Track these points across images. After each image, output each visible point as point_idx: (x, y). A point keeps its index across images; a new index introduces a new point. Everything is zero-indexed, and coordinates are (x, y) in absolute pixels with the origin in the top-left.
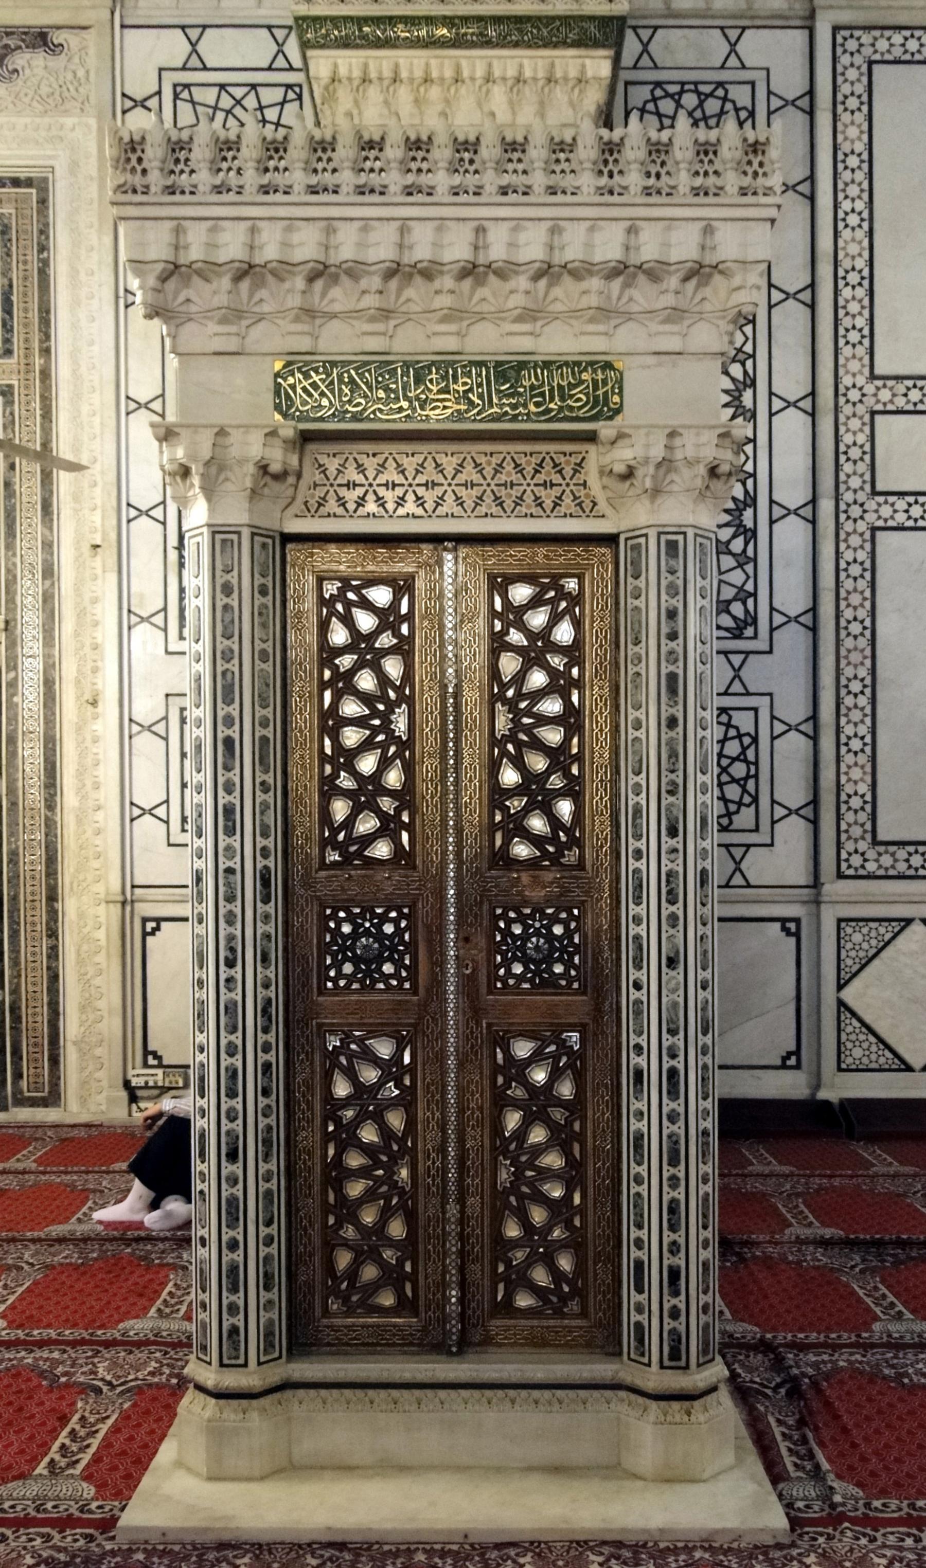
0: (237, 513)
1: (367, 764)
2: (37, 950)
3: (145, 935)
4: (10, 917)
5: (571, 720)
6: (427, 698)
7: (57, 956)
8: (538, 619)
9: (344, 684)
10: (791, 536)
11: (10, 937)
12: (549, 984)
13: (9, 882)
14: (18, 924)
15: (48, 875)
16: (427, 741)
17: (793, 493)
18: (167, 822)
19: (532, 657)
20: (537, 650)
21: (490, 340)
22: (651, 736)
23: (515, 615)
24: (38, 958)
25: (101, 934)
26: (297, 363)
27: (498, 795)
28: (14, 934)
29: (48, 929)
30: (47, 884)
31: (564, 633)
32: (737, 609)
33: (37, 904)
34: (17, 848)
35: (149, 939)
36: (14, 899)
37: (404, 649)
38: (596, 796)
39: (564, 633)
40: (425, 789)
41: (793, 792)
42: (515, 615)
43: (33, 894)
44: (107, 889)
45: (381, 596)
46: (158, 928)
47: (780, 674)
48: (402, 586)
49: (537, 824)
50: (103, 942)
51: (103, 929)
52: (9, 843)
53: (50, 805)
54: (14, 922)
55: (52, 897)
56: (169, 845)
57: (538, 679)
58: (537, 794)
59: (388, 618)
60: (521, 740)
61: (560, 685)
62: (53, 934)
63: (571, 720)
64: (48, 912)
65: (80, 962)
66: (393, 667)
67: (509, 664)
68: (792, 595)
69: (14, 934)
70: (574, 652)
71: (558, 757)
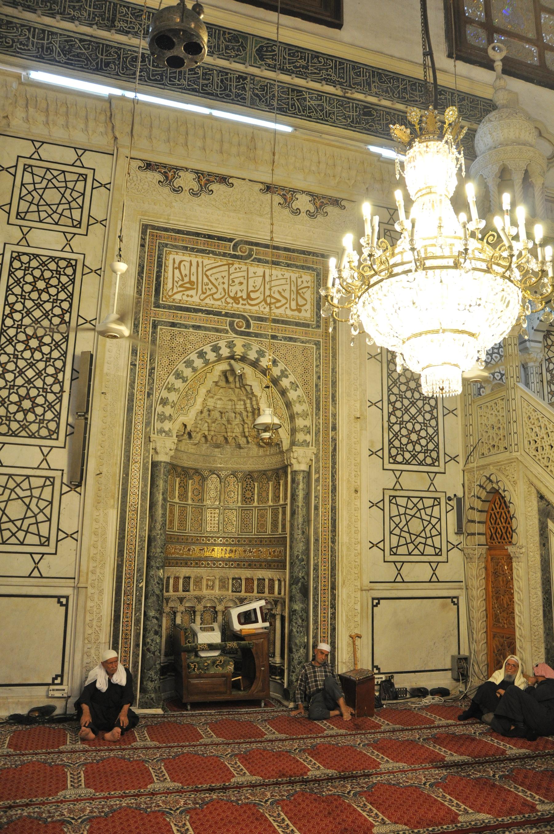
2: (326, 615)
3: (373, 606)
4: (314, 598)
7: (335, 618)
11: (313, 608)
13: (313, 580)
14: (318, 602)
15: (331, 576)
18: (384, 550)
24: (326, 619)
25: (358, 607)
28: (315, 607)
29: (331, 604)
30: (331, 581)
33: (326, 591)
34: (318, 562)
35: (375, 608)
36: (316, 589)
43: (325, 586)
44: (361, 584)
46: (378, 603)
50: (359, 611)
51: (359, 604)
52: (314, 560)
53: (333, 542)
54: (316, 601)
55: (333, 588)
56: (385, 562)
62: (333, 606)
64: (331, 595)
65: (348, 620)
69: (315, 607)
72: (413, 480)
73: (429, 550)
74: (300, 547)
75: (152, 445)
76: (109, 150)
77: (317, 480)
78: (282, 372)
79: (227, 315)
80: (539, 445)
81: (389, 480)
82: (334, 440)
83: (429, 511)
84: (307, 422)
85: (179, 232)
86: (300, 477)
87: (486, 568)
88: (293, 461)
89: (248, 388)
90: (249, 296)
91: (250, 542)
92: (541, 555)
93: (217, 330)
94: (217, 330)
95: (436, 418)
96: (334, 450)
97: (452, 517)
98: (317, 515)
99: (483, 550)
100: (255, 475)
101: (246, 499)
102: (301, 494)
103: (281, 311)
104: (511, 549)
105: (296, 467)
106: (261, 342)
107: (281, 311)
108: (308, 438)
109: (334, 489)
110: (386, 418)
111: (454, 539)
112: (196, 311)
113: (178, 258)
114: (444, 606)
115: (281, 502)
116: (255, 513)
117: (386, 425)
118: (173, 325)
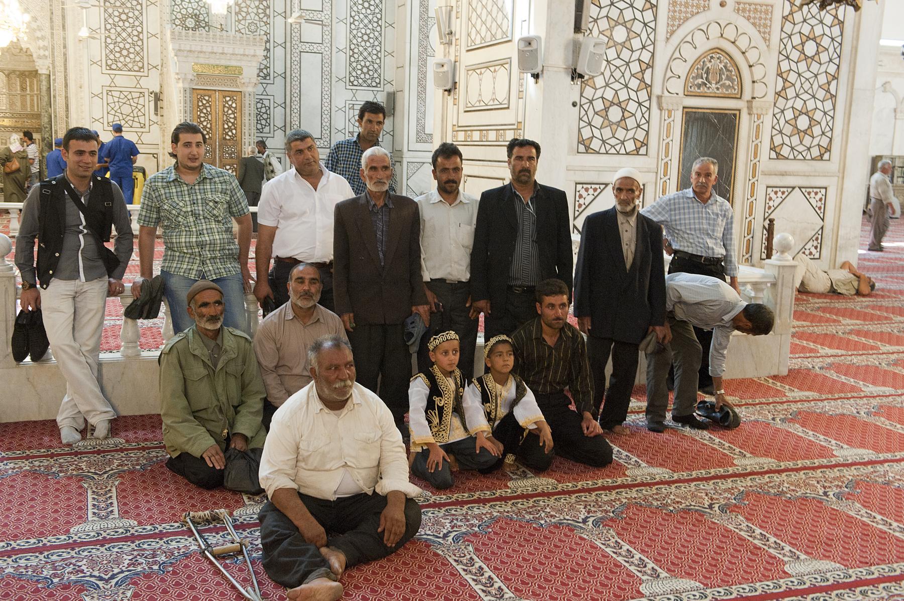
0: (187, 86)
1: (205, 124)
5: (235, 118)
6: (214, 114)
8: (230, 103)
9: (201, 111)
10: (279, 51)
12: (232, 158)
16: (214, 120)
17: (280, 40)
19: (229, 108)
20: (230, 107)
21: (224, 62)
22: (247, 121)
23: (227, 102)
26: (196, 64)
27: (224, 129)
31: (234, 105)
32: (265, 71)
37: (210, 106)
38: (239, 130)
39: (234, 105)
40: (214, 128)
41: (279, 123)
42: (227, 102)
45: (207, 98)
47: (276, 90)
48: (210, 97)
49: (230, 134)
57: (230, 112)
58: (230, 129)
59: (208, 101)
60: (228, 121)
61: (234, 113)
63: (235, 118)
66: (209, 109)
67: (226, 109)
68: (279, 69)
70: (235, 108)
71: (233, 124)
72: (124, 80)
73: (136, 124)
74: (46, 120)
77: (54, 80)
81: (106, 80)
82: (65, 54)
83: (136, 100)
84: (46, 43)
91: (28, 116)
95: (142, 40)
96: (66, 60)
97: (152, 104)
98: (55, 101)
100: (27, 73)
101: (23, 89)
102: (44, 88)
108: (47, 53)
109: (66, 86)
110: (103, 40)
111: (153, 117)
114: (147, 159)
116: (28, 97)
117: (103, 45)
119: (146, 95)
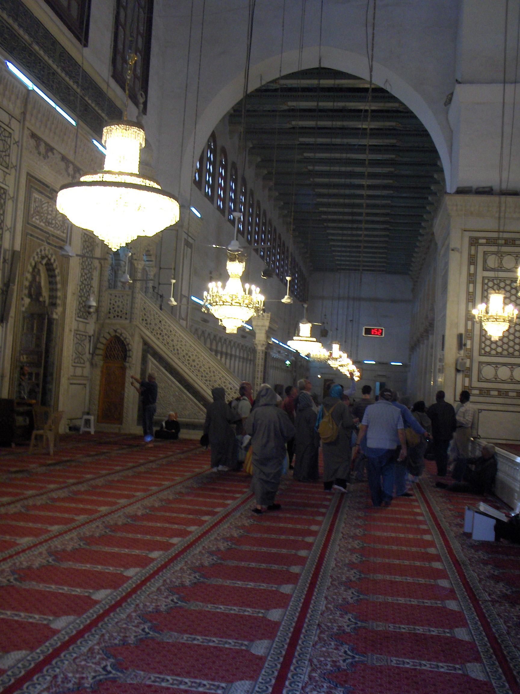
72: (81, 327)
75: (23, 302)
76: (19, 118)
78: (57, 266)
79: (45, 232)
80: (149, 321)
85: (36, 179)
86: (55, 322)
87: (102, 372)
88: (54, 314)
89: (36, 270)
90: (52, 224)
92: (141, 369)
93: (42, 241)
94: (42, 241)
99: (101, 363)
103: (58, 232)
104: (127, 365)
105: (55, 316)
106: (52, 249)
107: (58, 232)
112: (38, 228)
113: (36, 196)
115: (35, 331)
118: (31, 235)
119: (88, 337)
